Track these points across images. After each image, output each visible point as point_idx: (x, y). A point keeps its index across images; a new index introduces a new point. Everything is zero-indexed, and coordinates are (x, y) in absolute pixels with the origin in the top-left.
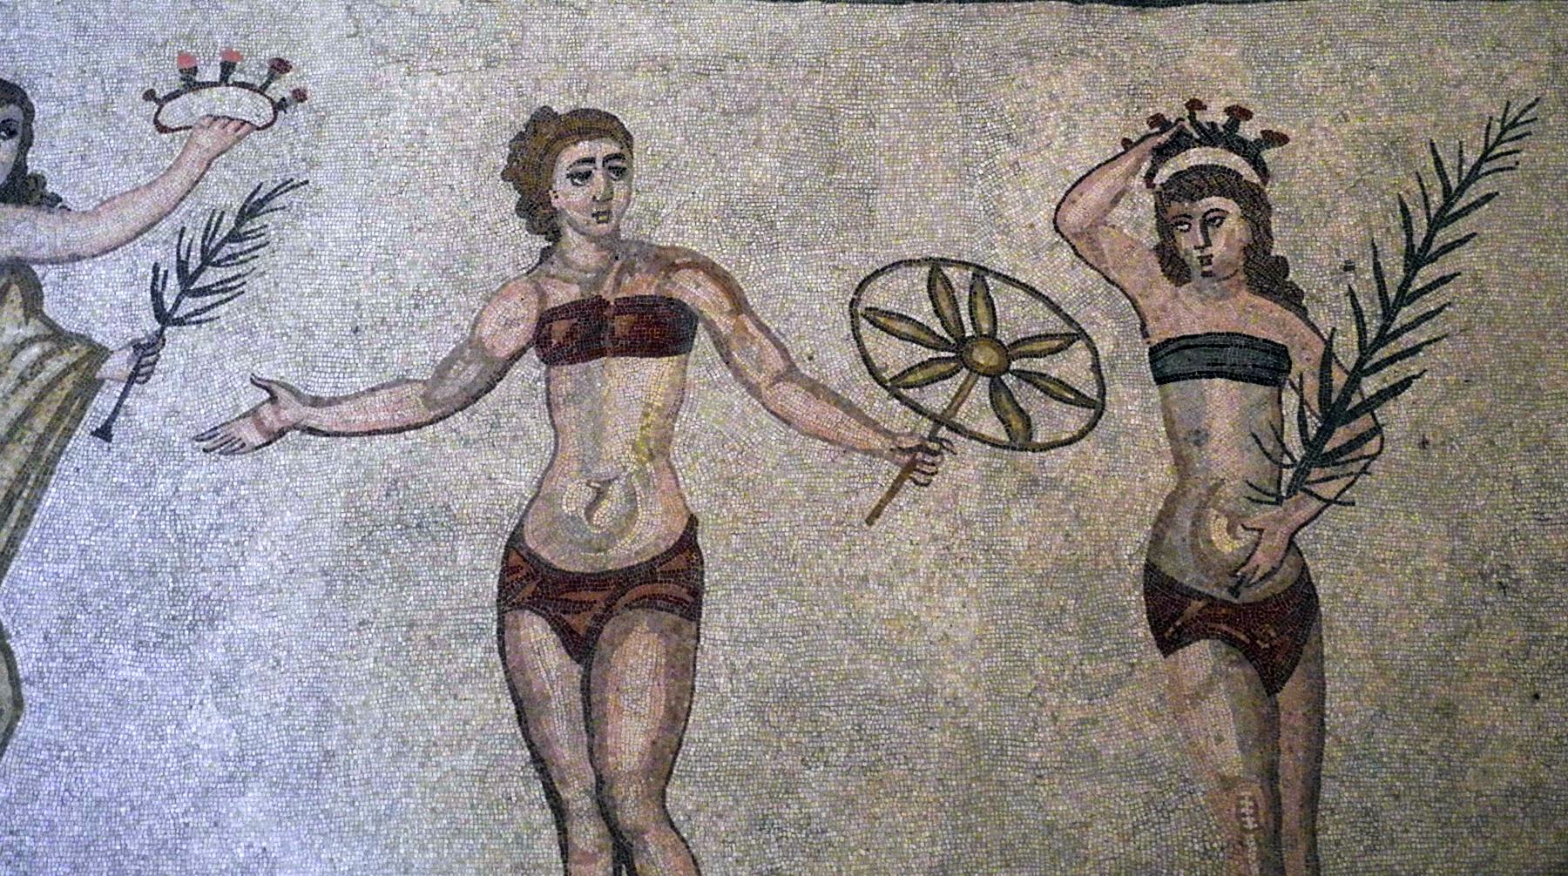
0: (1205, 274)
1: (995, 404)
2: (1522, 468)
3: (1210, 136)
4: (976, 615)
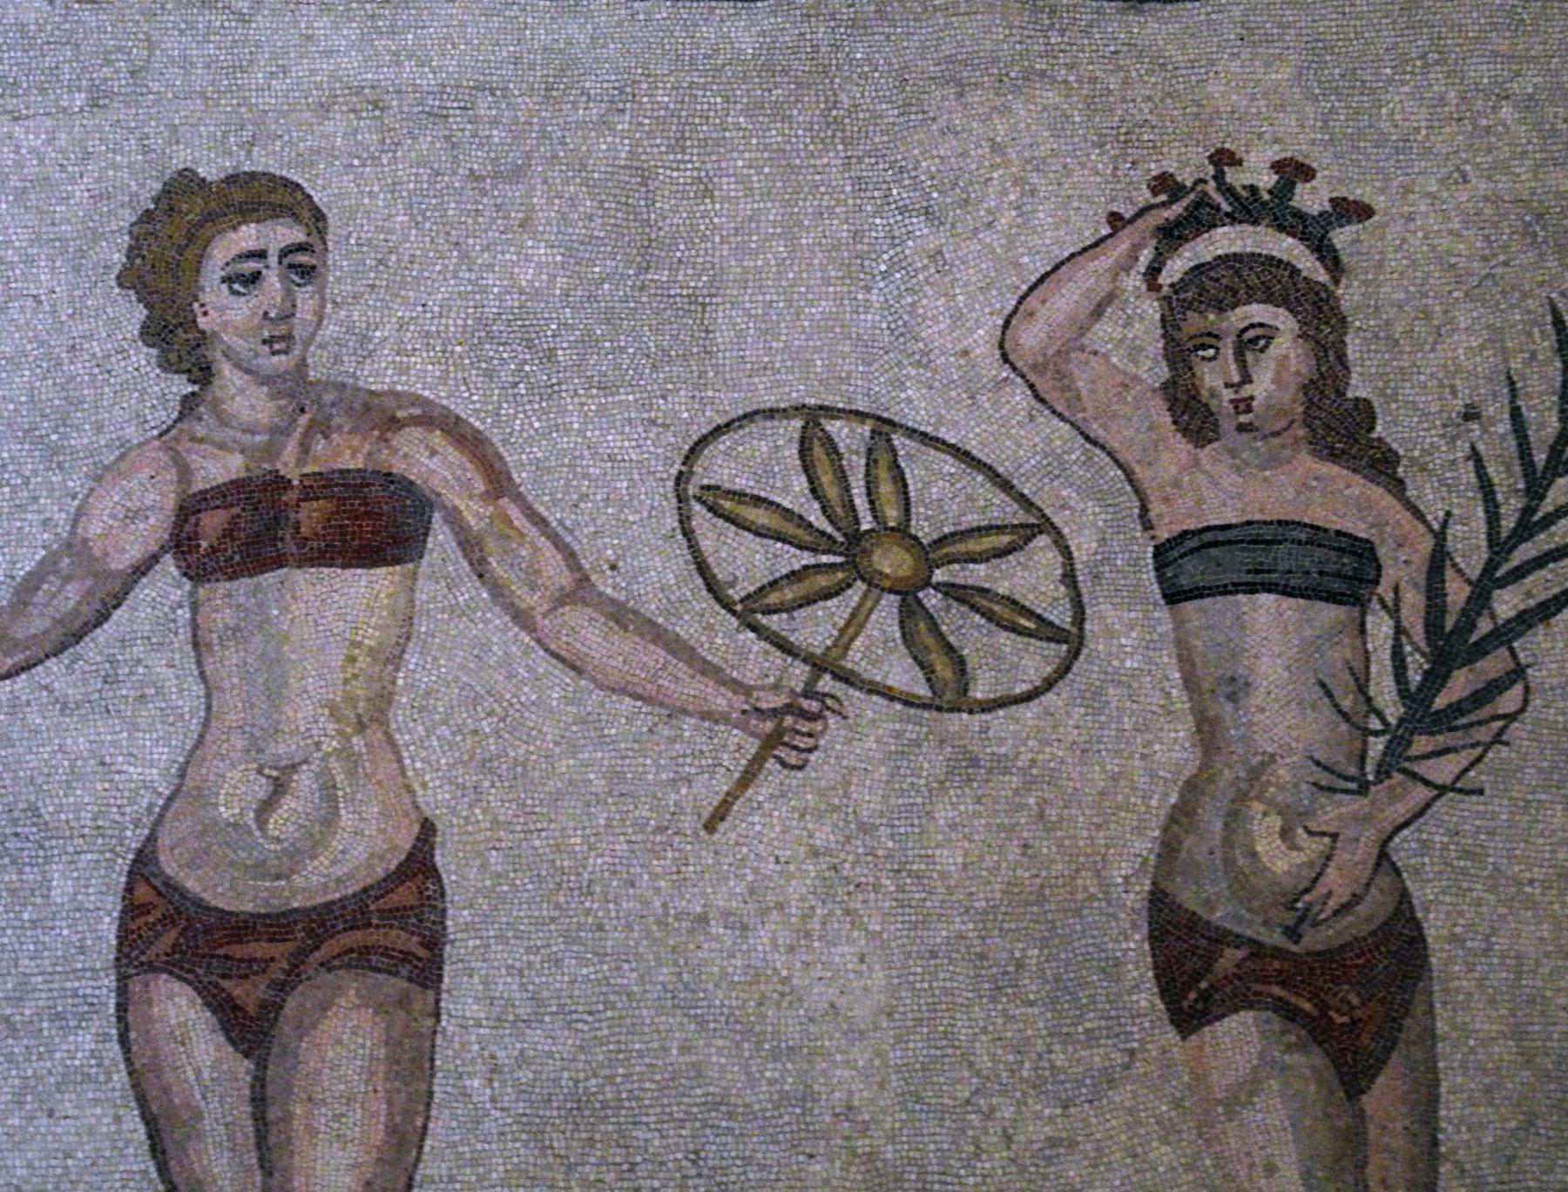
0: (1241, 428)
3: (1248, 208)
4: (881, 975)
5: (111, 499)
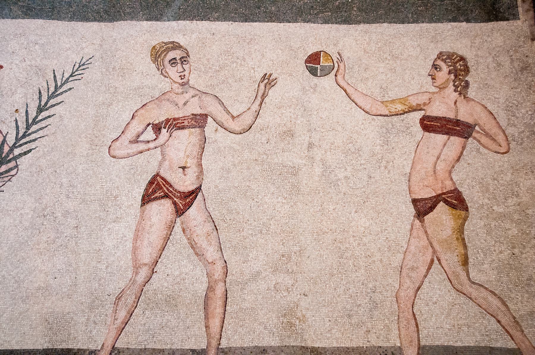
2: (64, 180)
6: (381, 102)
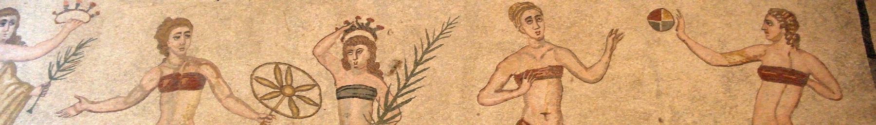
0: (355, 67)
1: (289, 105)
3: (361, 27)
5: (149, 77)
6: (720, 53)
